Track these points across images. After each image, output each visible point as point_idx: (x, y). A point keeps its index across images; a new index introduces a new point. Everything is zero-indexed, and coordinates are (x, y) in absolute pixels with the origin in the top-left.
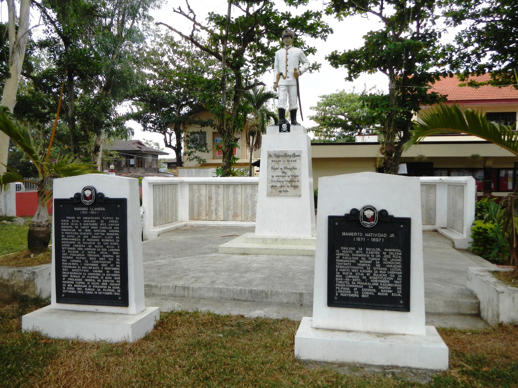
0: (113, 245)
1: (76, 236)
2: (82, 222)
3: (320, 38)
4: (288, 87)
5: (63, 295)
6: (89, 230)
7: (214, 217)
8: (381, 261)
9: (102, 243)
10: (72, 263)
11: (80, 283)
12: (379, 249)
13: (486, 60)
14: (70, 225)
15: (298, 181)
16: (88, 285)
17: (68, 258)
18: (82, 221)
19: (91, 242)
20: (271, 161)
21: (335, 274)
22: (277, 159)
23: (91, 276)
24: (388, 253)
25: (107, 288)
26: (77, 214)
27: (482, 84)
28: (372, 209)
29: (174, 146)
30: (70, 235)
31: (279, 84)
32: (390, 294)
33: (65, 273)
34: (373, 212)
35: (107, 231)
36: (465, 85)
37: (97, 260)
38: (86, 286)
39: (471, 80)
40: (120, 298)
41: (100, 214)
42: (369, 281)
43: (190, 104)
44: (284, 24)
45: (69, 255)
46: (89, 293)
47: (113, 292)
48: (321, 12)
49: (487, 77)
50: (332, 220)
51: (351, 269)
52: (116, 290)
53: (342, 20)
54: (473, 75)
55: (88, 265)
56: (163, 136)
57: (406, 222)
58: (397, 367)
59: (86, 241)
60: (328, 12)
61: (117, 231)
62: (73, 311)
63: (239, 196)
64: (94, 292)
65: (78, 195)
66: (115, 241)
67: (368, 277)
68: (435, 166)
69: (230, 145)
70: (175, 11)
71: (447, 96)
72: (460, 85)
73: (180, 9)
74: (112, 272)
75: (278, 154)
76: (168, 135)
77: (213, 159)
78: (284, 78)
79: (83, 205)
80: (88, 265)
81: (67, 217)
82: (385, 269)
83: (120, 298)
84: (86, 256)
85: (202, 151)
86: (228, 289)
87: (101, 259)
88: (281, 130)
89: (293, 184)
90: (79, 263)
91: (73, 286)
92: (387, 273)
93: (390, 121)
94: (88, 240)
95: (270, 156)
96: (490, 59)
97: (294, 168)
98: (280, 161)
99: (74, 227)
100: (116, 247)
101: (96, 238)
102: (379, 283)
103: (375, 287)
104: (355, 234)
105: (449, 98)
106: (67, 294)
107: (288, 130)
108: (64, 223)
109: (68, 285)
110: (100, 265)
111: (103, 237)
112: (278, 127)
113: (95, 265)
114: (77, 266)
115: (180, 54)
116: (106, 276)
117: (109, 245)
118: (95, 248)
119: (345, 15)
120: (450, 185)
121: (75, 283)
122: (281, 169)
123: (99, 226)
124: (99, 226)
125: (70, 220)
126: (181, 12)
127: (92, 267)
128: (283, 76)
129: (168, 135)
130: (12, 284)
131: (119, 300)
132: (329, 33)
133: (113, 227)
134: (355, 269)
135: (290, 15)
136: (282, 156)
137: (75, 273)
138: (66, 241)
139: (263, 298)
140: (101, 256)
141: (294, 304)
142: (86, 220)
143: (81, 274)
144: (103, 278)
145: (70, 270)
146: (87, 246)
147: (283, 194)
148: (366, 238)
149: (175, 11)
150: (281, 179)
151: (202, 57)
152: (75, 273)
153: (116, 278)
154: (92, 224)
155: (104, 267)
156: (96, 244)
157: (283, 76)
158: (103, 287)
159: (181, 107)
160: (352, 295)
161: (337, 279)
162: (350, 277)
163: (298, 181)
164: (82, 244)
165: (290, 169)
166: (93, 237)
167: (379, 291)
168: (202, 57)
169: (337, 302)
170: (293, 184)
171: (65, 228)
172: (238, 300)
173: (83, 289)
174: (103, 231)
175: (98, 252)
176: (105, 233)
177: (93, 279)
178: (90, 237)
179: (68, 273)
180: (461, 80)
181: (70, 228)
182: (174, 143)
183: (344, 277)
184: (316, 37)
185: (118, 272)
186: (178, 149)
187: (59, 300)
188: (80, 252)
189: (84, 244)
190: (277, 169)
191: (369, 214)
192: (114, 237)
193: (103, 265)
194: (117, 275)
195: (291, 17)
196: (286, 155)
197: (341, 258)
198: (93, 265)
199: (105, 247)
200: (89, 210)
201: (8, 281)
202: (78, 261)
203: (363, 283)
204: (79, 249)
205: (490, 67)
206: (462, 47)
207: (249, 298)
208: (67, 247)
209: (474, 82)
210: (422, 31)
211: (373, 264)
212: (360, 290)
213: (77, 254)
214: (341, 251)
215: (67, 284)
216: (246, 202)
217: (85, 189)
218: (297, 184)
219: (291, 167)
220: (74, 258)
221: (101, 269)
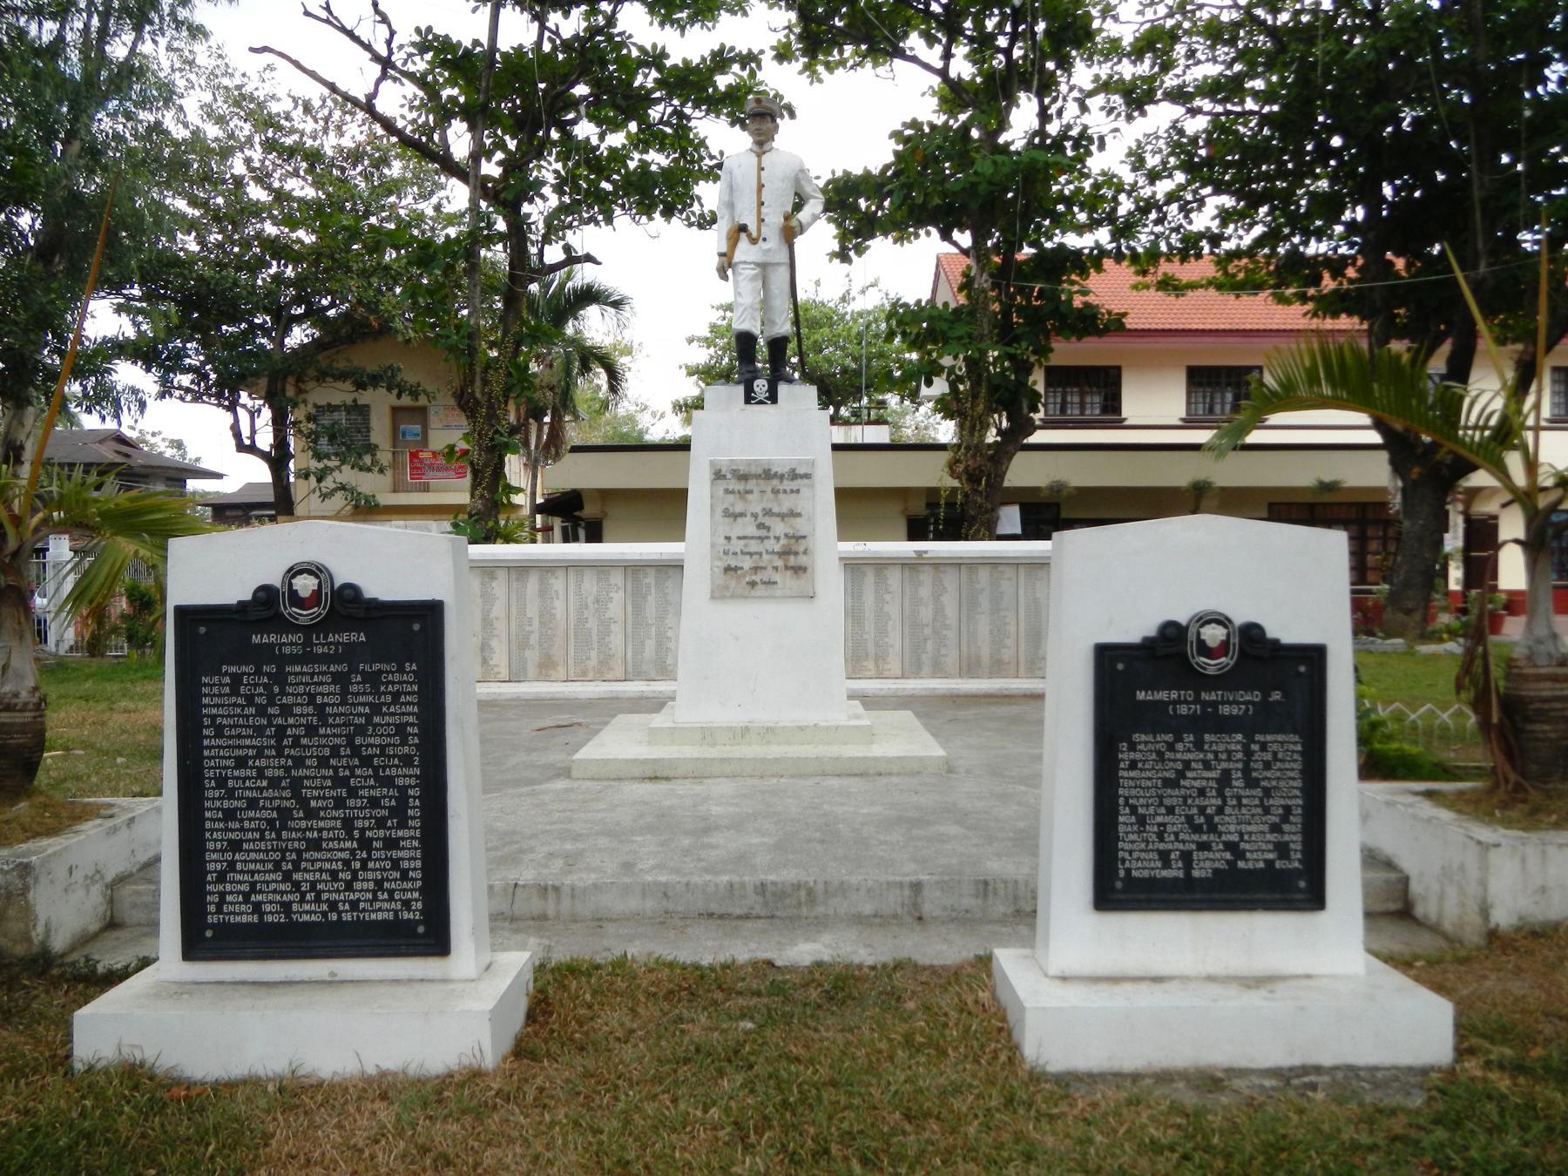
0: (394, 756)
1: (259, 731)
2: (283, 684)
4: (764, 267)
5: (209, 934)
6: (310, 709)
8: (1246, 771)
9: (356, 751)
10: (241, 821)
11: (272, 886)
12: (1239, 737)
13: (1203, 220)
14: (235, 692)
15: (805, 552)
16: (303, 895)
17: (226, 804)
18: (280, 678)
20: (721, 492)
21: (1117, 813)
23: (313, 861)
24: (1264, 747)
25: (375, 899)
27: (1192, 286)
28: (1222, 621)
29: (267, 449)
30: (235, 726)
31: (736, 259)
32: (1269, 863)
33: (215, 856)
34: (1224, 631)
35: (376, 709)
36: (1147, 287)
37: (336, 807)
38: (296, 897)
39: (1165, 274)
40: (421, 929)
41: (349, 653)
42: (1213, 828)
43: (314, 315)
44: (646, 79)
45: (230, 794)
46: (306, 918)
47: (396, 912)
48: (762, 52)
49: (1202, 269)
50: (1106, 655)
51: (1161, 797)
52: (407, 904)
53: (820, 81)
54: (1169, 260)
55: (303, 824)
56: (228, 418)
57: (1315, 656)
58: (1318, 1069)
59: (296, 743)
60: (783, 55)
61: (410, 709)
62: (243, 983)
63: (559, 605)
64: (324, 914)
65: (266, 594)
66: (404, 743)
67: (1209, 819)
68: (1064, 515)
69: (494, 447)
70: (307, 13)
71: (1124, 315)
72: (1135, 287)
73: (328, 8)
74: (391, 844)
75: (743, 469)
76: (243, 415)
77: (395, 491)
78: (754, 241)
79: (289, 626)
80: (303, 824)
81: (224, 668)
82: (1258, 792)
83: (421, 929)
84: (296, 794)
85: (361, 469)
86: (687, 884)
87: (351, 803)
88: (749, 399)
89: (792, 560)
90: (271, 822)
91: (247, 900)
92: (1262, 805)
93: (976, 384)
94: (304, 741)
95: (718, 475)
96: (1213, 218)
97: (794, 514)
98: (750, 492)
99: (250, 700)
100: (407, 761)
101: (334, 735)
102: (1241, 835)
103: (1230, 846)
104: (1174, 695)
105: (1130, 323)
107: (773, 397)
108: (213, 690)
109: (229, 898)
110: (348, 824)
111: (361, 730)
112: (741, 389)
113: (331, 824)
114: (262, 832)
115: (290, 153)
116: (369, 858)
117: (383, 754)
118: (329, 767)
119: (830, 67)
121: (253, 889)
122: (755, 516)
123: (344, 692)
124: (344, 692)
125: (236, 680)
126: (331, 20)
127: (320, 830)
128: (749, 236)
129: (243, 415)
131: (416, 935)
133: (396, 696)
134: (1173, 797)
135: (664, 55)
136: (758, 477)
137: (253, 856)
138: (219, 747)
139: (800, 904)
140: (353, 793)
141: (895, 916)
142: (296, 674)
143: (276, 856)
144: (358, 865)
145: (235, 846)
146: (299, 762)
147: (760, 590)
148: (1205, 704)
149: (307, 13)
150: (754, 546)
151: (360, 168)
152: (253, 856)
153: (405, 865)
154: (321, 689)
155: (363, 830)
156: (335, 751)
157: (749, 236)
158: (357, 895)
159: (284, 324)
160: (1165, 873)
161: (1121, 828)
162: (1159, 819)
163: (805, 552)
164: (280, 755)
165: (782, 516)
166: (322, 731)
168: (360, 168)
169: (1120, 896)
170: (792, 560)
171: (217, 706)
172: (721, 917)
174: (360, 709)
175: (339, 782)
176: (369, 717)
177: (321, 870)
178: (311, 731)
179: (229, 856)
180: (1137, 273)
181: (235, 705)
182: (265, 440)
183: (1142, 821)
185: (415, 843)
186: (278, 459)
187: (194, 948)
188: (274, 783)
189: (288, 757)
190: (742, 515)
191: (1213, 635)
192: (401, 729)
193: (359, 824)
194: (411, 855)
195: (668, 63)
196: (767, 475)
197: (1133, 765)
198: (321, 824)
199: (366, 762)
200: (308, 643)
202: (266, 814)
203: (1196, 837)
204: (269, 773)
205: (1215, 240)
206: (1142, 181)
207: (758, 910)
208: (226, 768)
209: (1172, 278)
210: (1053, 128)
211: (1225, 780)
212: (1187, 857)
213: (261, 789)
214: (1133, 747)
215: (222, 895)
216: (582, 621)
217: (294, 572)
218: (803, 560)
219: (784, 510)
220: (253, 804)
221: (352, 838)
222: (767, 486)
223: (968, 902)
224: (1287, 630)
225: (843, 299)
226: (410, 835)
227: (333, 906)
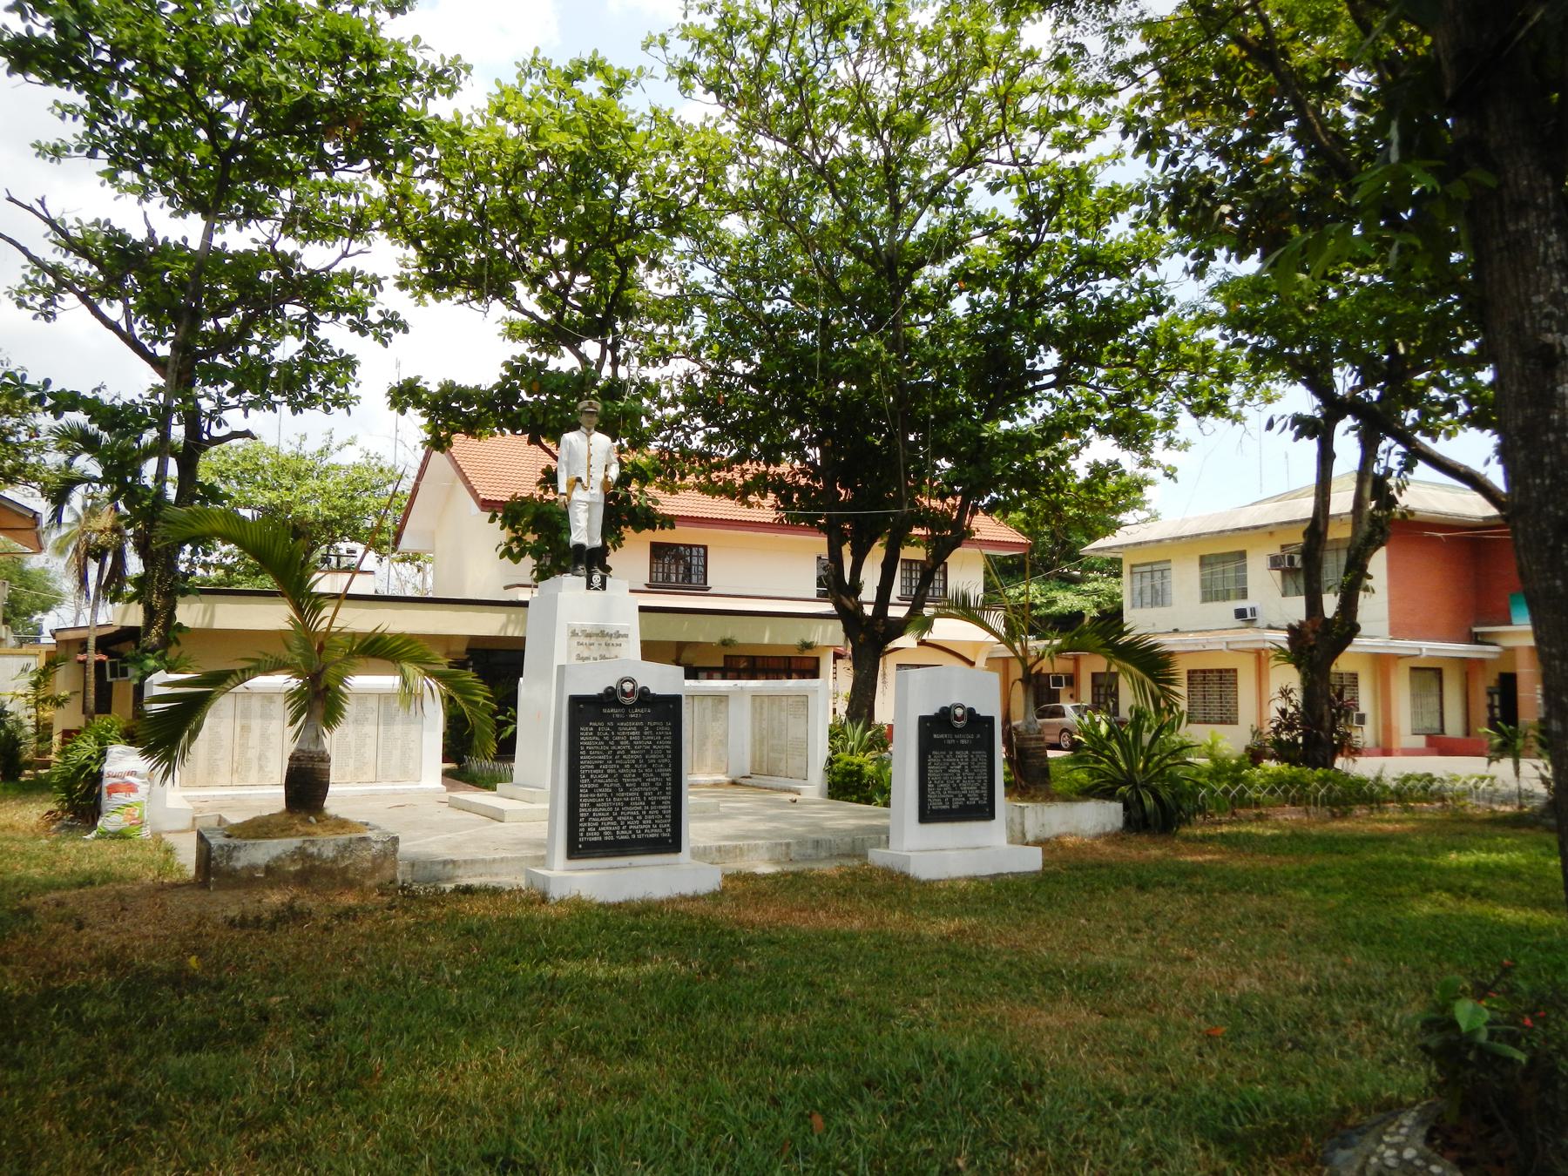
1: (605, 752)
3: (371, 336)
7: (253, 779)
9: (646, 761)
18: (615, 728)
19: (629, 759)
22: (587, 641)
26: (606, 718)
28: (962, 707)
35: (654, 742)
50: (923, 720)
57: (991, 720)
70: (11, 199)
73: (42, 203)
74: (659, 803)
78: (585, 489)
88: (589, 586)
95: (574, 634)
100: (666, 765)
103: (965, 796)
106: (588, 845)
107: (603, 586)
110: (641, 794)
111: (648, 752)
112: (584, 580)
125: (596, 728)
130: (343, 865)
132: (396, 330)
140: (644, 780)
145: (593, 805)
146: (622, 766)
149: (11, 199)
173: (614, 833)
175: (638, 775)
178: (627, 752)
184: (363, 333)
188: (611, 776)
191: (959, 712)
192: (664, 751)
194: (666, 808)
196: (603, 634)
199: (650, 766)
201: (334, 860)
205: (703, 456)
217: (624, 681)
220: (601, 785)
222: (603, 641)
224: (982, 711)
226: (667, 799)
227: (634, 831)
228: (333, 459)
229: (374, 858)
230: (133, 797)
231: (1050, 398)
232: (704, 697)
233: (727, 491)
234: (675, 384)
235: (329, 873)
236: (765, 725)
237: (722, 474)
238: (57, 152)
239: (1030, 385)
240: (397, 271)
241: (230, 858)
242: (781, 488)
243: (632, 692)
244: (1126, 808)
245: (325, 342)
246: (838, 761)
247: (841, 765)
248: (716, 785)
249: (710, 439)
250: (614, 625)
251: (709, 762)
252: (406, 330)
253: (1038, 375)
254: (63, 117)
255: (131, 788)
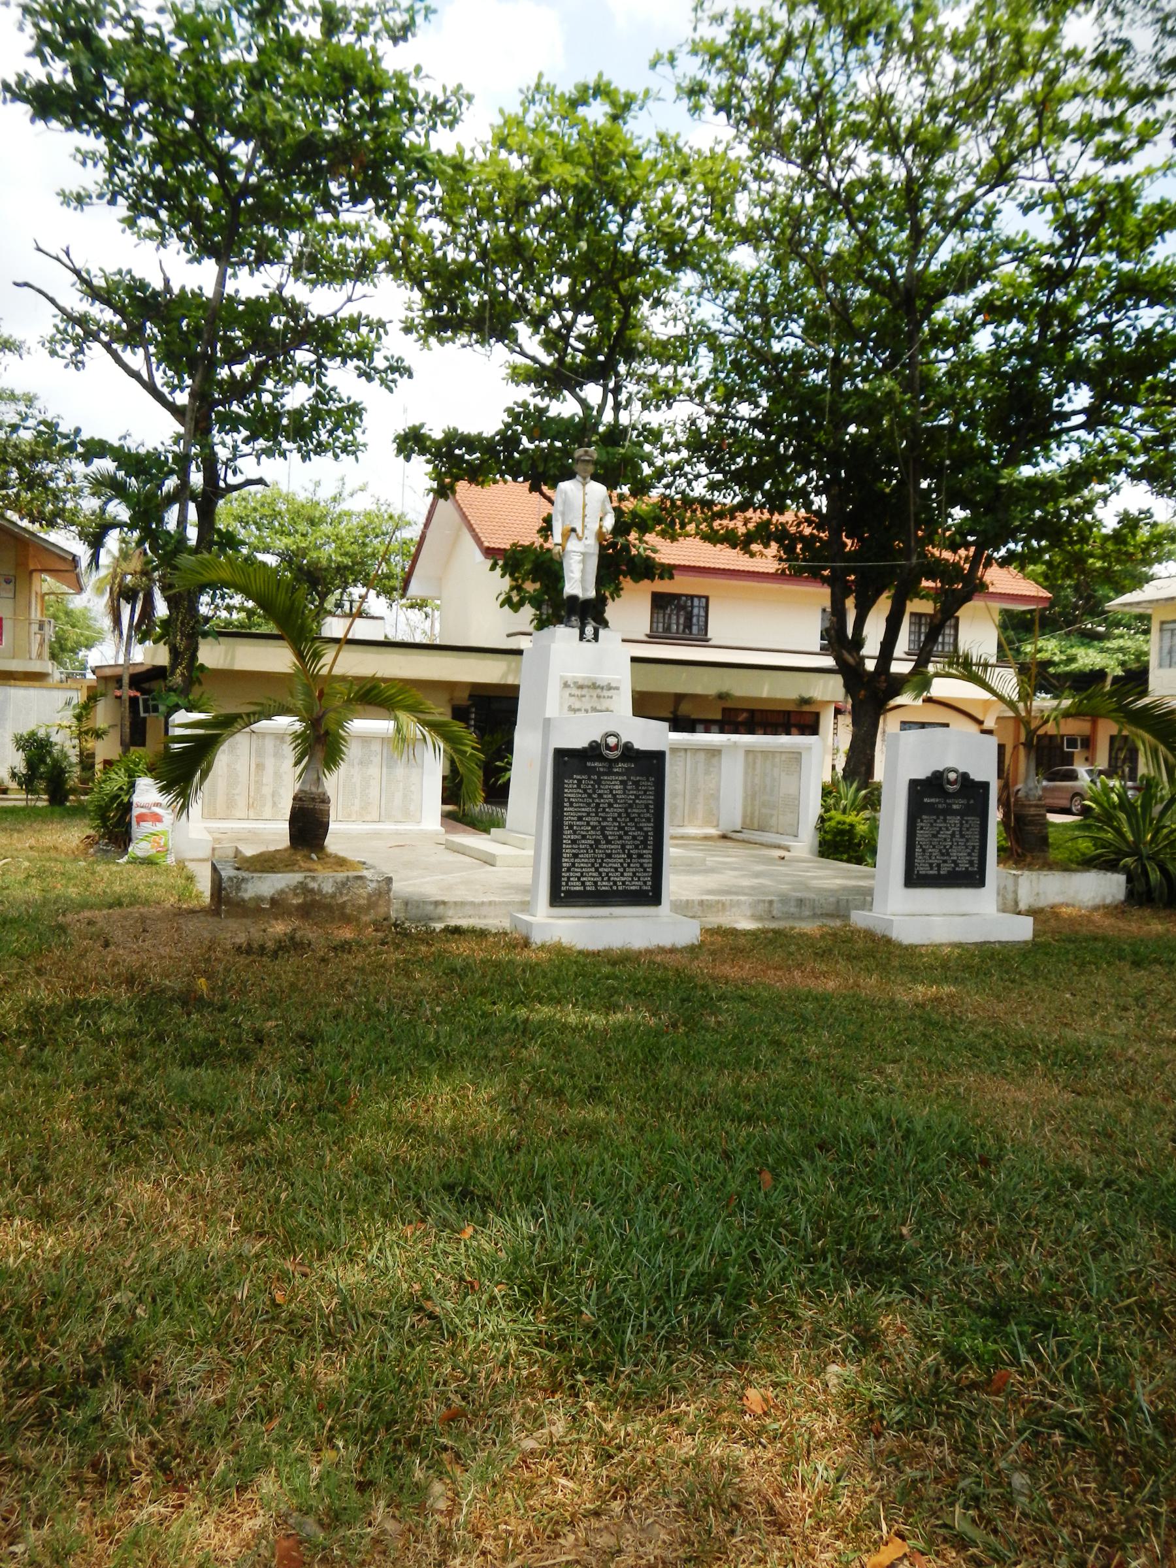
1: (589, 805)
3: (377, 382)
9: (628, 815)
18: (599, 782)
22: (579, 692)
26: (589, 771)
28: (955, 771)
35: (637, 797)
42: (948, 854)
50: (913, 783)
57: (985, 786)
70: (39, 249)
73: (68, 254)
74: (640, 856)
75: (581, 682)
78: (580, 539)
88: (581, 638)
95: (566, 685)
99: (585, 790)
100: (648, 820)
103: (954, 862)
106: (568, 893)
107: (596, 638)
110: (623, 847)
111: (631, 806)
112: (577, 631)
120: (749, 752)
125: (580, 781)
130: (340, 901)
132: (401, 375)
140: (626, 833)
145: (575, 856)
146: (605, 819)
149: (39, 249)
156: (620, 814)
167: (957, 865)
173: (595, 883)
175: (620, 828)
178: (610, 805)
183: (924, 851)
184: (370, 379)
188: (594, 828)
191: (952, 776)
192: (647, 806)
194: (648, 862)
196: (594, 686)
199: (632, 820)
201: (333, 896)
212: (938, 866)
220: (584, 837)
222: (594, 693)
223: (793, 910)
224: (977, 776)
225: (334, 499)
227: (615, 883)
228: (345, 506)
229: (370, 896)
230: (159, 827)
231: (1078, 441)
232: (697, 750)
233: (730, 539)
234: (678, 428)
235: (329, 908)
236: (757, 780)
237: (725, 522)
238: (80, 200)
239: (1056, 427)
240: (403, 314)
241: (238, 889)
242: (782, 536)
243: (616, 747)
244: (1129, 880)
245: (334, 389)
246: (830, 819)
247: (833, 823)
248: (707, 838)
249: (713, 486)
250: (604, 677)
251: (700, 814)
252: (411, 376)
253: (1066, 416)
254: (84, 164)
255: (157, 818)
